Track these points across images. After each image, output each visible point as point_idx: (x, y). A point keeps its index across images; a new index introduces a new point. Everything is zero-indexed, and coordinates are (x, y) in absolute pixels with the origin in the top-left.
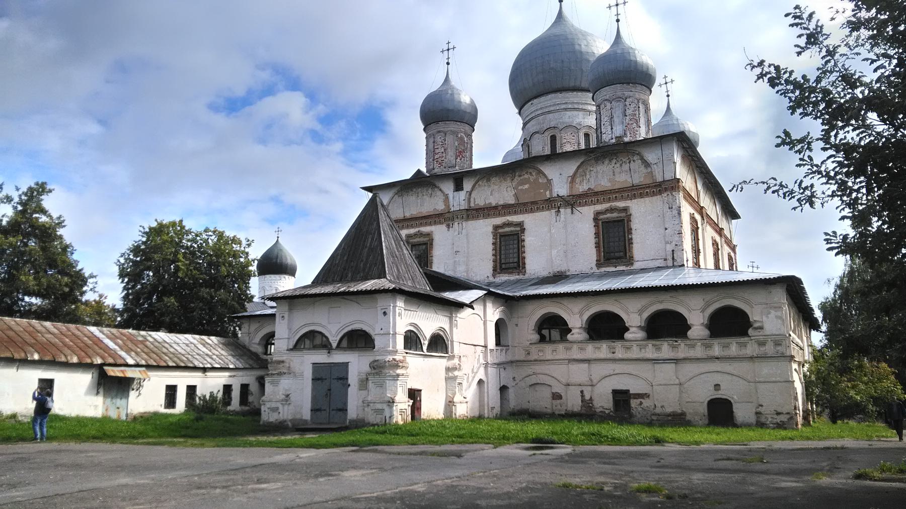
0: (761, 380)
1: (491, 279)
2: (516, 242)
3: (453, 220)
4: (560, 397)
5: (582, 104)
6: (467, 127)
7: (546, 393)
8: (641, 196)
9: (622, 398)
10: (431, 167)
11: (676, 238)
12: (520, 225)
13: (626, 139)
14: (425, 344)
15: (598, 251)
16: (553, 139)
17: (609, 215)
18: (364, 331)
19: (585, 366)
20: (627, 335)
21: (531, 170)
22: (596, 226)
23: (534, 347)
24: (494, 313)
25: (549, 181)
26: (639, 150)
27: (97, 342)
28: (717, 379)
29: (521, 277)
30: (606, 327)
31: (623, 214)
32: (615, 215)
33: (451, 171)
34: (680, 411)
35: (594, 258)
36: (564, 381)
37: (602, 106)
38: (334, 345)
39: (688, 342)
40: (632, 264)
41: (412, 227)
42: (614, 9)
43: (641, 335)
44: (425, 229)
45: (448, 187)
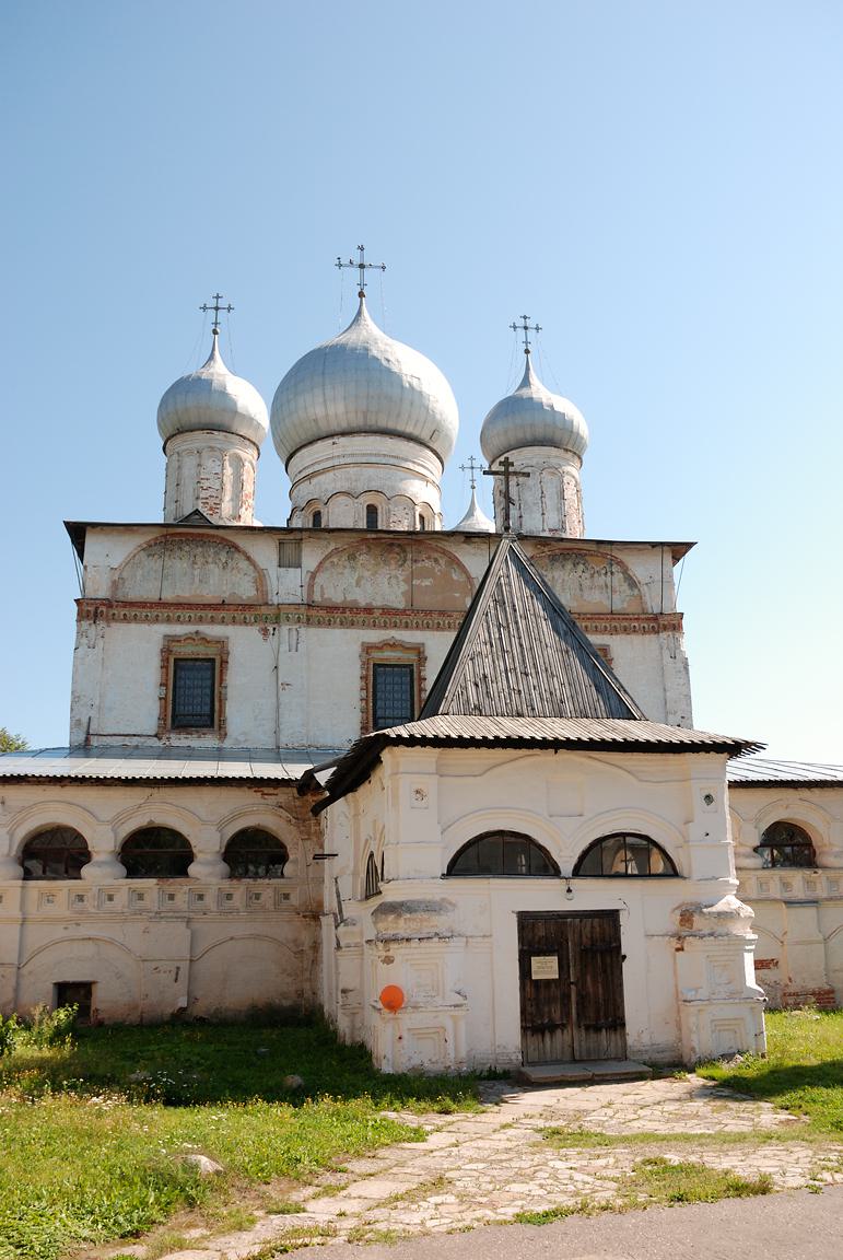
3: (277, 620)
5: (419, 465)
8: (626, 630)
16: (372, 511)
21: (436, 555)
34: (827, 987)
38: (567, 867)
41: (178, 620)
42: (521, 332)
44: (213, 631)
45: (265, 553)
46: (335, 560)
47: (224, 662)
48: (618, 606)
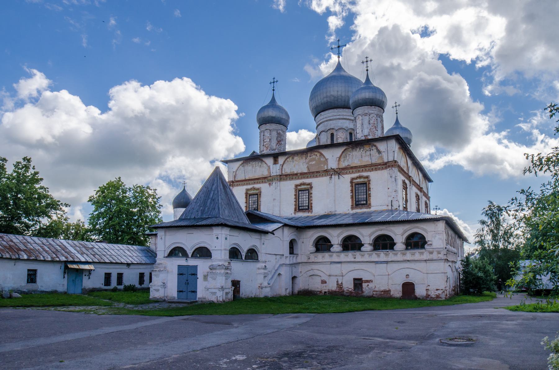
0: (430, 272)
1: (293, 215)
2: (307, 194)
4: (326, 282)
6: (283, 127)
7: (318, 280)
8: (376, 169)
9: (358, 283)
10: (262, 150)
11: (394, 193)
12: (310, 184)
13: (370, 137)
14: (244, 254)
15: (352, 200)
16: (332, 135)
17: (358, 180)
18: (206, 248)
19: (339, 265)
20: (363, 249)
21: (316, 153)
22: (352, 186)
23: (312, 255)
24: (288, 235)
25: (327, 160)
26: (376, 144)
27: (64, 248)
28: (407, 272)
29: (310, 214)
30: (351, 244)
31: (366, 180)
32: (362, 180)
33: (273, 152)
35: (350, 204)
36: (328, 273)
37: (357, 118)
39: (394, 252)
40: (370, 208)
41: (249, 184)
43: (370, 248)
44: (257, 186)
45: (270, 161)
46: (288, 160)
47: (260, 195)
48: (374, 162)
